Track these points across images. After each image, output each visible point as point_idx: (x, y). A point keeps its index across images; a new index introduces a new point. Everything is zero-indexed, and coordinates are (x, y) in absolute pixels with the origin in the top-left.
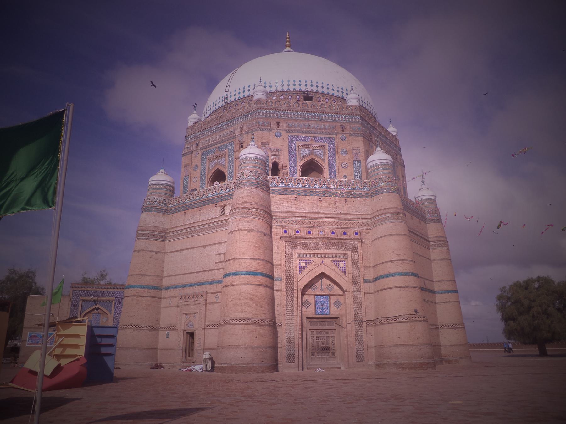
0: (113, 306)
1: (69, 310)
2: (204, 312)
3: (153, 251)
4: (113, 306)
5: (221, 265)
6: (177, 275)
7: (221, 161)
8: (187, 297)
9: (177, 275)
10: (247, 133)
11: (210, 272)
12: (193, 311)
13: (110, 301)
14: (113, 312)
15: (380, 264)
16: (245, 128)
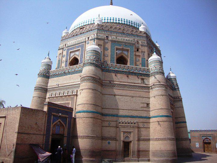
0: (67, 121)
1: (46, 121)
2: (136, 132)
3: (100, 92)
4: (67, 121)
5: (145, 109)
6: (113, 109)
7: (126, 53)
8: (124, 123)
9: (113, 109)
10: (142, 46)
11: (138, 112)
12: (129, 131)
13: (66, 118)
14: (67, 125)
15: (179, 117)
16: (140, 42)
